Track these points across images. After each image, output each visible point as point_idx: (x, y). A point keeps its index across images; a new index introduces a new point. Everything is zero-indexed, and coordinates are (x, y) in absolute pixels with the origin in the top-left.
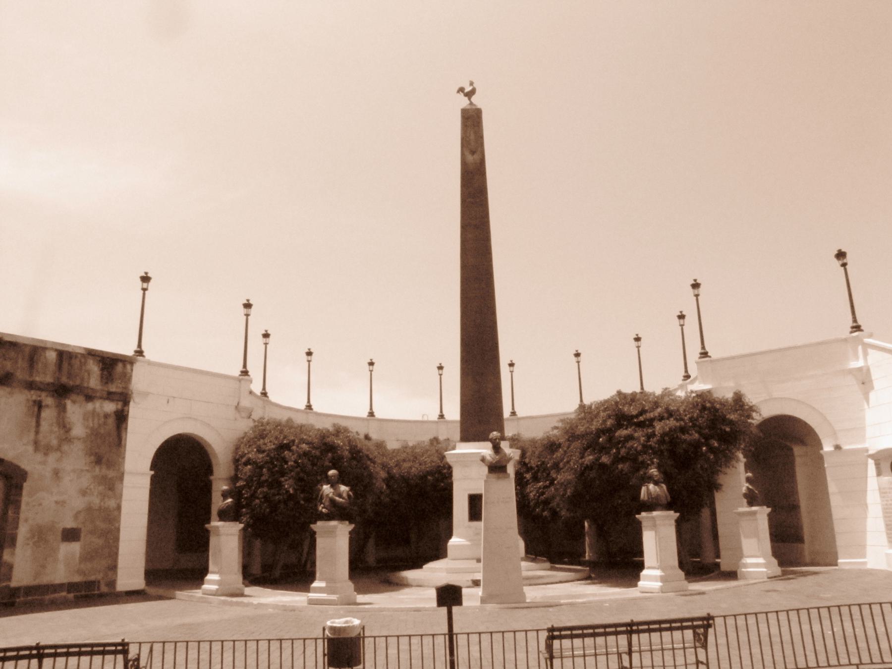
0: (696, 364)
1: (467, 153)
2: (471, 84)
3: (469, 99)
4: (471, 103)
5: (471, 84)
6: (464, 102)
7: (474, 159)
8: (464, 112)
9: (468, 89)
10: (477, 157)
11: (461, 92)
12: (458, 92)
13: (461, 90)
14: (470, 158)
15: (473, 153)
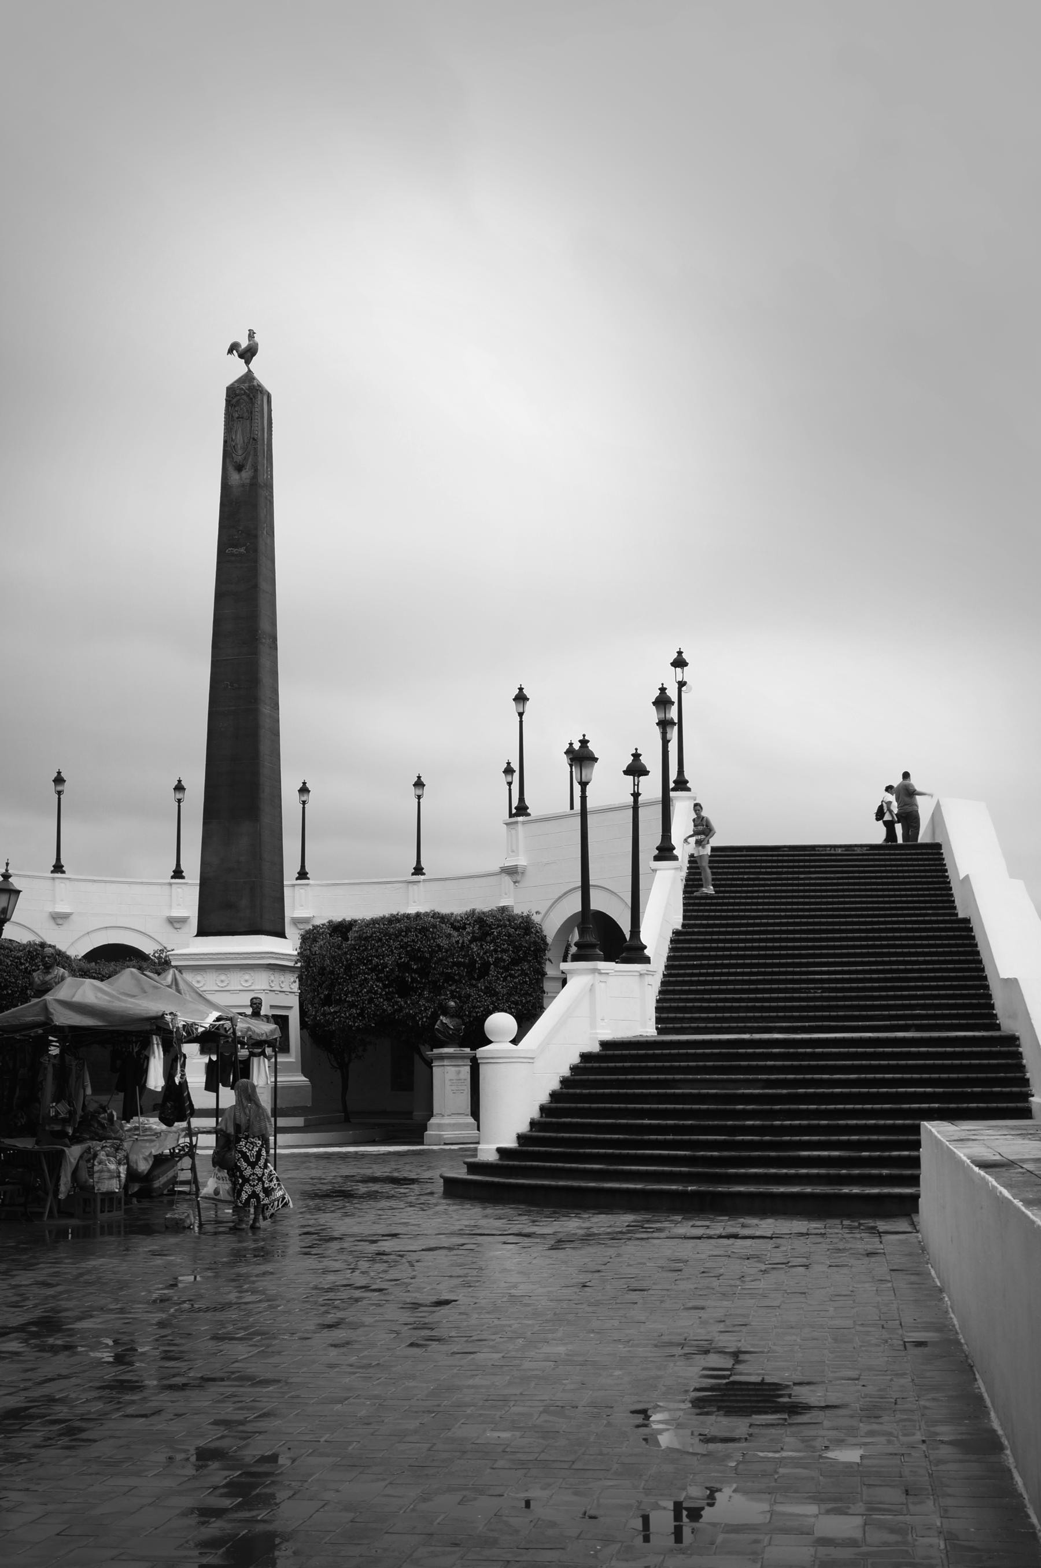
0: (505, 826)
1: (231, 469)
2: (251, 335)
3: (247, 363)
4: (249, 371)
5: (251, 335)
6: (237, 368)
7: (241, 479)
8: (233, 394)
9: (244, 344)
10: (246, 474)
11: (234, 352)
12: (230, 351)
13: (233, 347)
14: (235, 477)
15: (239, 468)
